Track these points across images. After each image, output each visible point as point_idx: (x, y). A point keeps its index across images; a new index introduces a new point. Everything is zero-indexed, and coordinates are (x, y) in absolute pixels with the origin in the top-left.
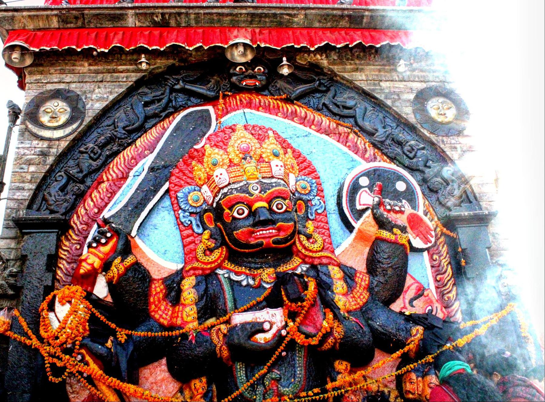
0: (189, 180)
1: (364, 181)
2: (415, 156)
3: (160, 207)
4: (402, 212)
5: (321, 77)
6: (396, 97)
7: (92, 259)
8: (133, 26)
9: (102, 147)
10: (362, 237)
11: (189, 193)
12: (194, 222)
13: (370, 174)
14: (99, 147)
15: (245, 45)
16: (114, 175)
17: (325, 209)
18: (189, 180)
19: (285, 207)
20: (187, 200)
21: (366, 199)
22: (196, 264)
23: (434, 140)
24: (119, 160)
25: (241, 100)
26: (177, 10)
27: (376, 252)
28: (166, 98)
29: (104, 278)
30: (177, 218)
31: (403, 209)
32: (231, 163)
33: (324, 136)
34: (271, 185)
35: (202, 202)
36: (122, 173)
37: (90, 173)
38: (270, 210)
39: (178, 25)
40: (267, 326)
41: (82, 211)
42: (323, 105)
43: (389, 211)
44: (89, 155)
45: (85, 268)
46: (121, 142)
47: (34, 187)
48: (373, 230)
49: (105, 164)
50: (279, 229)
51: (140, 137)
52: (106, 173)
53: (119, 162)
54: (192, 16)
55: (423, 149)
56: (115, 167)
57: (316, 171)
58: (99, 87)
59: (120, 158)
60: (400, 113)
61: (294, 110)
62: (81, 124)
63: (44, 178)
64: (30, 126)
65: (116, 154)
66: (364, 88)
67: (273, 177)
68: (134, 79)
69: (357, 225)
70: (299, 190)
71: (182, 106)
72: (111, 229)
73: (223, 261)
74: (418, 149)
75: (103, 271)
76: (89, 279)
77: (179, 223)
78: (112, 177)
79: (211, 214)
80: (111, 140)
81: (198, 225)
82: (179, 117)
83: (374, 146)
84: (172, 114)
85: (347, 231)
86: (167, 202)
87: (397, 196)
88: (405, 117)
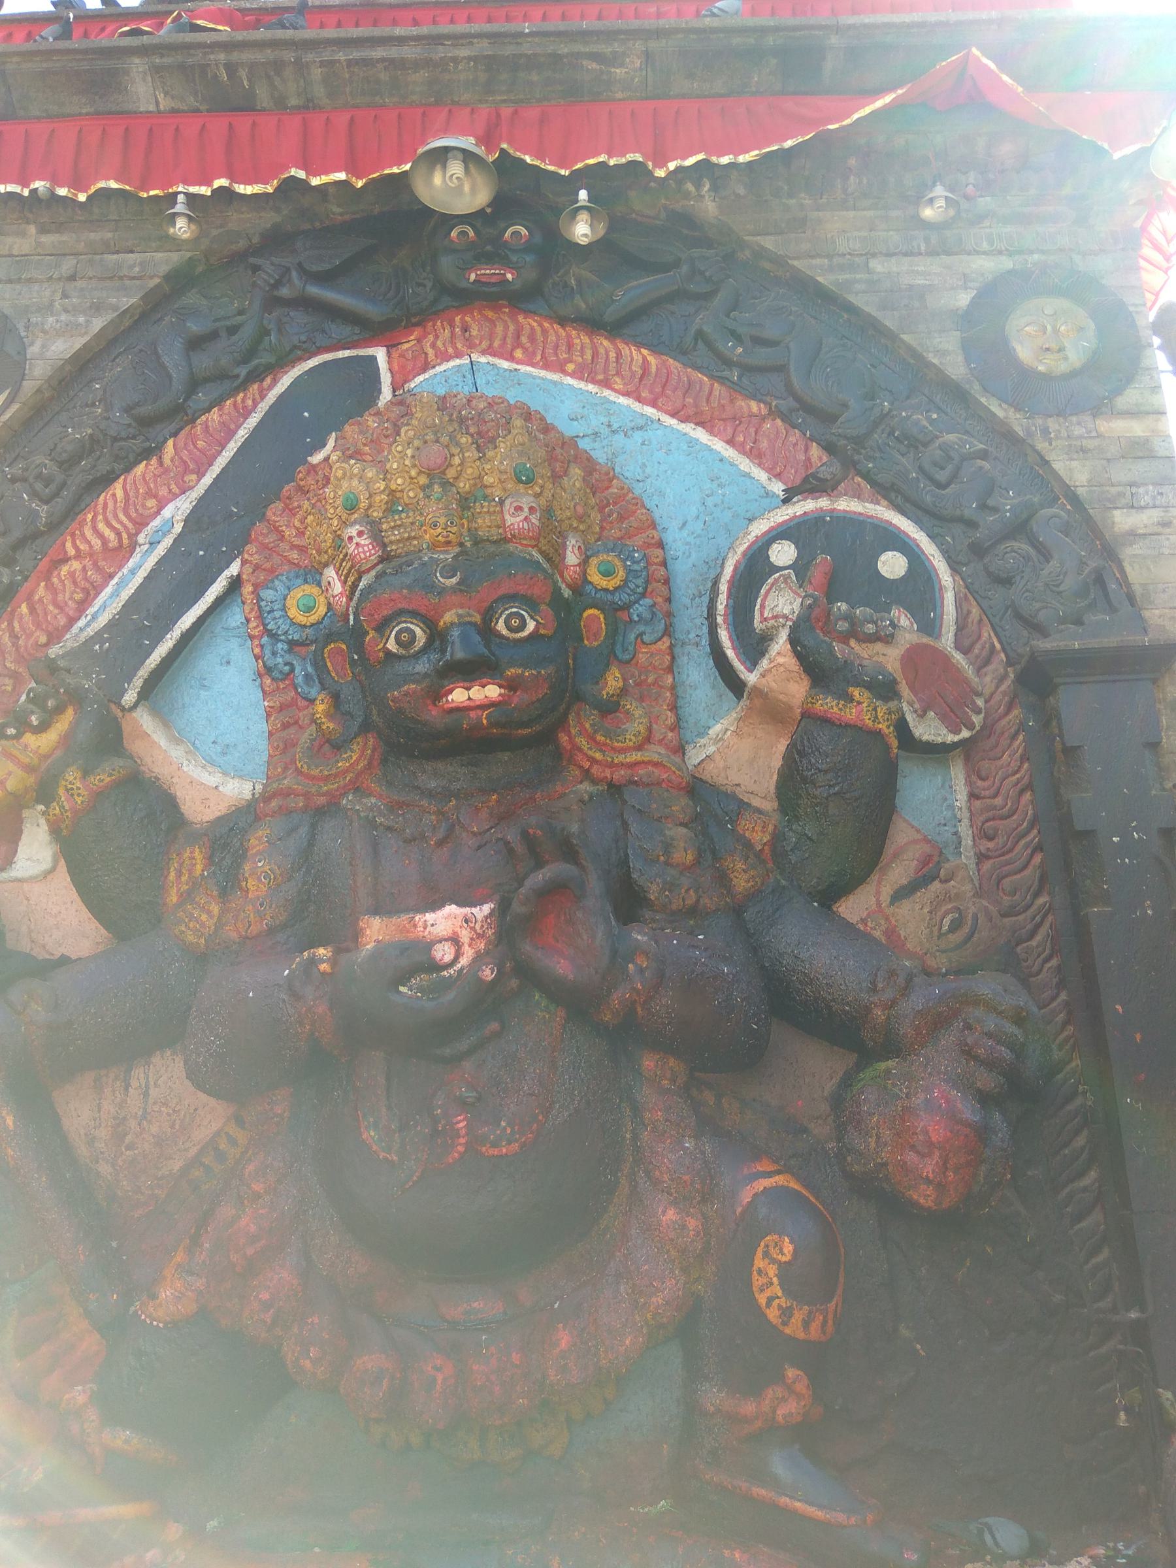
0: (294, 555)
1: (783, 554)
2: (954, 477)
3: (218, 629)
4: (888, 639)
5: (696, 252)
8: (152, 108)
9: (68, 464)
10: (767, 709)
12: (298, 670)
14: (60, 464)
15: (468, 157)
16: (97, 543)
18: (294, 555)
19: (531, 626)
20: (284, 609)
23: (1018, 429)
25: (465, 329)
26: (269, 54)
27: (799, 752)
29: (42, 821)
30: (257, 658)
33: (688, 428)
35: (322, 610)
36: (119, 534)
39: (280, 102)
42: (696, 340)
43: (844, 638)
44: (31, 486)
46: (121, 449)
48: (797, 690)
49: (72, 512)
50: (511, 686)
51: (175, 434)
52: (73, 535)
53: (110, 505)
54: (317, 73)
55: (984, 455)
56: (100, 517)
57: (653, 525)
58: (65, 296)
59: (114, 495)
60: (919, 349)
61: (612, 355)
66: (819, 279)
67: (506, 540)
68: (164, 269)
70: (595, 577)
71: (299, 348)
74: (965, 458)
75: (38, 801)
78: (91, 547)
79: (344, 647)
81: (307, 676)
82: (286, 381)
85: (730, 694)
86: (235, 617)
88: (935, 361)
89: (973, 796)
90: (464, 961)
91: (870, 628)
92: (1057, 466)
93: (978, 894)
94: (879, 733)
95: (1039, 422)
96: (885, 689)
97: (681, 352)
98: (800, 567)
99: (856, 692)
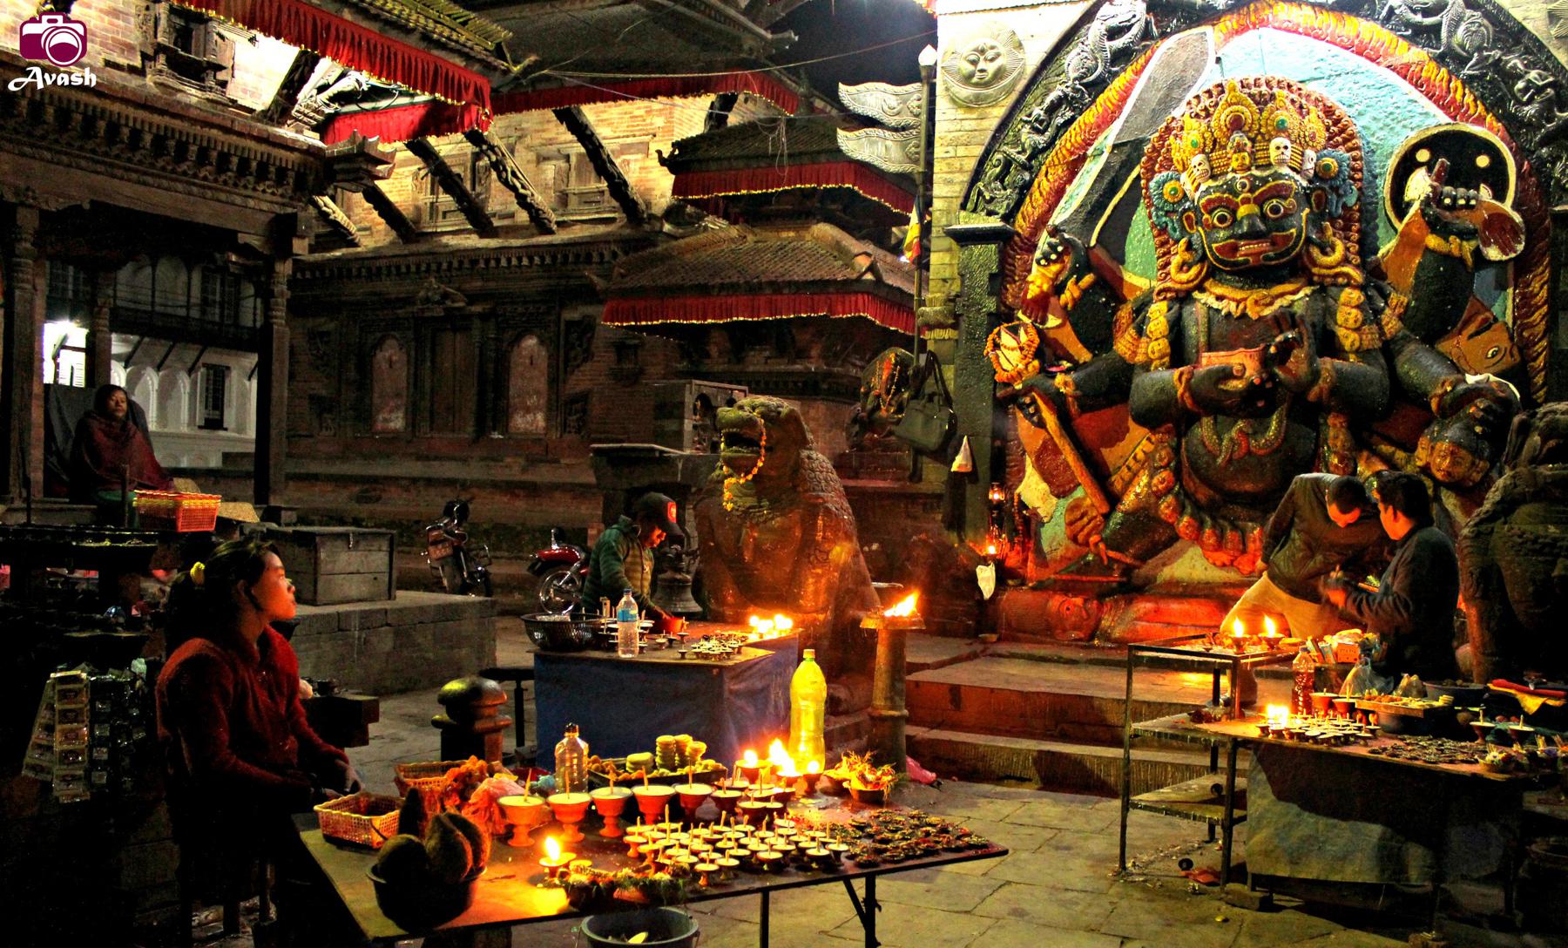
1: (1423, 155)
9: (1053, 109)
11: (1164, 182)
13: (1437, 143)
21: (1419, 185)
22: (1169, 284)
31: (1473, 202)
34: (1264, 180)
38: (1263, 217)
45: (1033, 291)
47: (966, 178)
65: (1072, 120)
67: (1269, 165)
69: (1400, 227)
72: (1064, 242)
73: (1203, 281)
77: (1153, 226)
87: (1471, 178)
91: (1462, 202)
94: (1461, 260)
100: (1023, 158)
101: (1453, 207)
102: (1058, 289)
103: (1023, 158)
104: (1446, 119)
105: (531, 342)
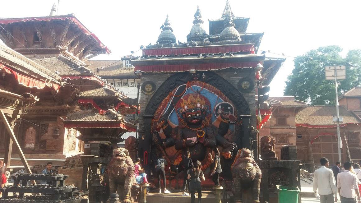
1: (220, 107)
4: (228, 115)
6: (234, 81)
7: (159, 125)
9: (160, 97)
10: (218, 120)
17: (211, 113)
24: (164, 100)
28: (175, 83)
32: (188, 104)
37: (158, 103)
38: (196, 115)
40: (193, 141)
41: (156, 113)
45: (158, 127)
48: (221, 119)
62: (155, 91)
63: (148, 105)
64: (143, 91)
69: (217, 118)
76: (159, 129)
80: (162, 95)
83: (226, 95)
84: (176, 87)
87: (228, 110)
89: (235, 127)
90: (195, 142)
91: (226, 114)
92: (245, 98)
93: (235, 135)
95: (244, 93)
96: (227, 119)
97: (213, 85)
98: (221, 108)
99: (225, 119)
100: (156, 104)
101: (225, 114)
102: (162, 127)
103: (156, 104)
104: (223, 101)
105: (32, 128)
